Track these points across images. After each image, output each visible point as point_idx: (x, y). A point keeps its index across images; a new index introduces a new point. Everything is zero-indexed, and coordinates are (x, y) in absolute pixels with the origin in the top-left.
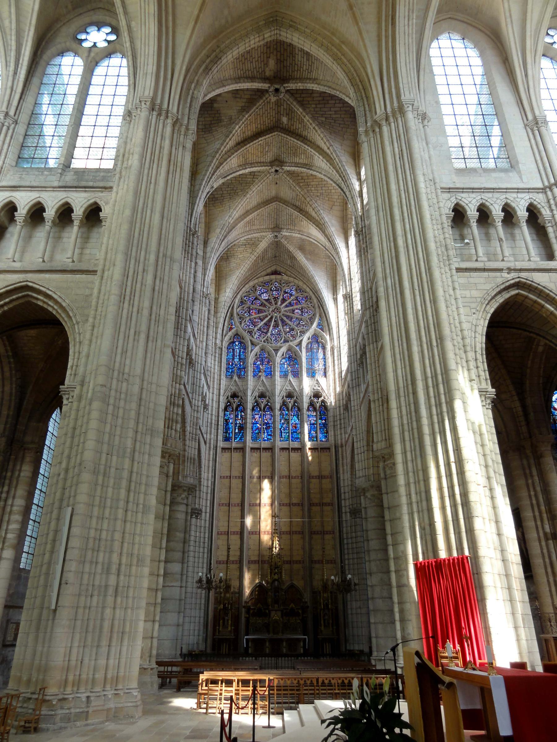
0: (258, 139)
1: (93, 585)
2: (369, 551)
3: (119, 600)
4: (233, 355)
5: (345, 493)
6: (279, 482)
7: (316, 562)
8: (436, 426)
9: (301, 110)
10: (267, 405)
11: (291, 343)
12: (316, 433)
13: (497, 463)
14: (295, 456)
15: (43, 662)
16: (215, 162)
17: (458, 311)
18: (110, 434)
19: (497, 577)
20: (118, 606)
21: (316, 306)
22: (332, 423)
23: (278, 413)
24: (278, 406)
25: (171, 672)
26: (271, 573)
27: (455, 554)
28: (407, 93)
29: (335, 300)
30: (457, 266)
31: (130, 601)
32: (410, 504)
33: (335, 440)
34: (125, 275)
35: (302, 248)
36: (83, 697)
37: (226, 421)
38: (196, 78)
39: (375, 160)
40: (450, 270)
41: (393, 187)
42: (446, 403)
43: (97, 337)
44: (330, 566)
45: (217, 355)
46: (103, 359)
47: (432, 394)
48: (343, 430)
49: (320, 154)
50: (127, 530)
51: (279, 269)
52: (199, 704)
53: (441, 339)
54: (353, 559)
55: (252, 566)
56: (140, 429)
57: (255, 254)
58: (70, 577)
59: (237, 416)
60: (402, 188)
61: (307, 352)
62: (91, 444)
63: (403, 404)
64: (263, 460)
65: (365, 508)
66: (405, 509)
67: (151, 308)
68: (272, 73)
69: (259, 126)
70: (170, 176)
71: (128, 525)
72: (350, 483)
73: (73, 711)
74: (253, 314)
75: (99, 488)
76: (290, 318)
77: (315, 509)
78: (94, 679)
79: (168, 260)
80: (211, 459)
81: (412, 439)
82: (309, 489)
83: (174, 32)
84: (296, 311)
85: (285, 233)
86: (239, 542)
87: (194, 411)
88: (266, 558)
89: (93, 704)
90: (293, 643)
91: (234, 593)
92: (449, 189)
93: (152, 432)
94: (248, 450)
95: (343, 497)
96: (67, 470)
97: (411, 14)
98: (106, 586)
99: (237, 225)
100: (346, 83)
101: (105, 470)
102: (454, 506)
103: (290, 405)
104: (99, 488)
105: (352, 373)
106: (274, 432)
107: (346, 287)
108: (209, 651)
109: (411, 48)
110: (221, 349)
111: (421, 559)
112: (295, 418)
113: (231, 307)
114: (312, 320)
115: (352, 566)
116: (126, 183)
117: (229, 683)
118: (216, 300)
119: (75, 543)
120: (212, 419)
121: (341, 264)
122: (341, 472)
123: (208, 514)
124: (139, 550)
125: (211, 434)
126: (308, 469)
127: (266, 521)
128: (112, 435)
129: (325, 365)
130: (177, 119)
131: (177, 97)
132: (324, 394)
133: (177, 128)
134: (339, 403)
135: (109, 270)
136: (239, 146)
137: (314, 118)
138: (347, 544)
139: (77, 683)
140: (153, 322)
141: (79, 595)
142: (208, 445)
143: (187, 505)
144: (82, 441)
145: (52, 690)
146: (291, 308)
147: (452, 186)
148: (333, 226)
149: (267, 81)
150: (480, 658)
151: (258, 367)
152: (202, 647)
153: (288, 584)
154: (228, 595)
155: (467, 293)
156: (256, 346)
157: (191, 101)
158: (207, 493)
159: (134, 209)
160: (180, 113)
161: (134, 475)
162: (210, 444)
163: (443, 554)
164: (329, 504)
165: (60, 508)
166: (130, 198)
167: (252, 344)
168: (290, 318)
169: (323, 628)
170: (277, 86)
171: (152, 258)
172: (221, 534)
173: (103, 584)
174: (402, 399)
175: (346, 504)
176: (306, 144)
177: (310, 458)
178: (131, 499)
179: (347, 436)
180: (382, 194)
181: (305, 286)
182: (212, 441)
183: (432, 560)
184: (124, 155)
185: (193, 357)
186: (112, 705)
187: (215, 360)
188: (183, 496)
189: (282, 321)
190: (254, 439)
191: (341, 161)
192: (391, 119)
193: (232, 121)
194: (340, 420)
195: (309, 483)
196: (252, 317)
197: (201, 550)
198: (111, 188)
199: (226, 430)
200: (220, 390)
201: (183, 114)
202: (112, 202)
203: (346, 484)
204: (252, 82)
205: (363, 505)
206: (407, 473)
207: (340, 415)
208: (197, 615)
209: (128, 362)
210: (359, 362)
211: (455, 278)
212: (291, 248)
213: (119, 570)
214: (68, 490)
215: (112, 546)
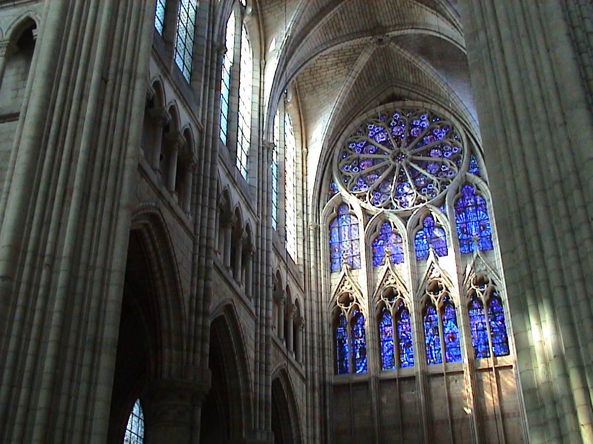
51: (397, 91)
80: (317, 405)
84: (433, 151)
120: (312, 342)
125: (313, 364)
181: (442, 111)
189: (412, 170)
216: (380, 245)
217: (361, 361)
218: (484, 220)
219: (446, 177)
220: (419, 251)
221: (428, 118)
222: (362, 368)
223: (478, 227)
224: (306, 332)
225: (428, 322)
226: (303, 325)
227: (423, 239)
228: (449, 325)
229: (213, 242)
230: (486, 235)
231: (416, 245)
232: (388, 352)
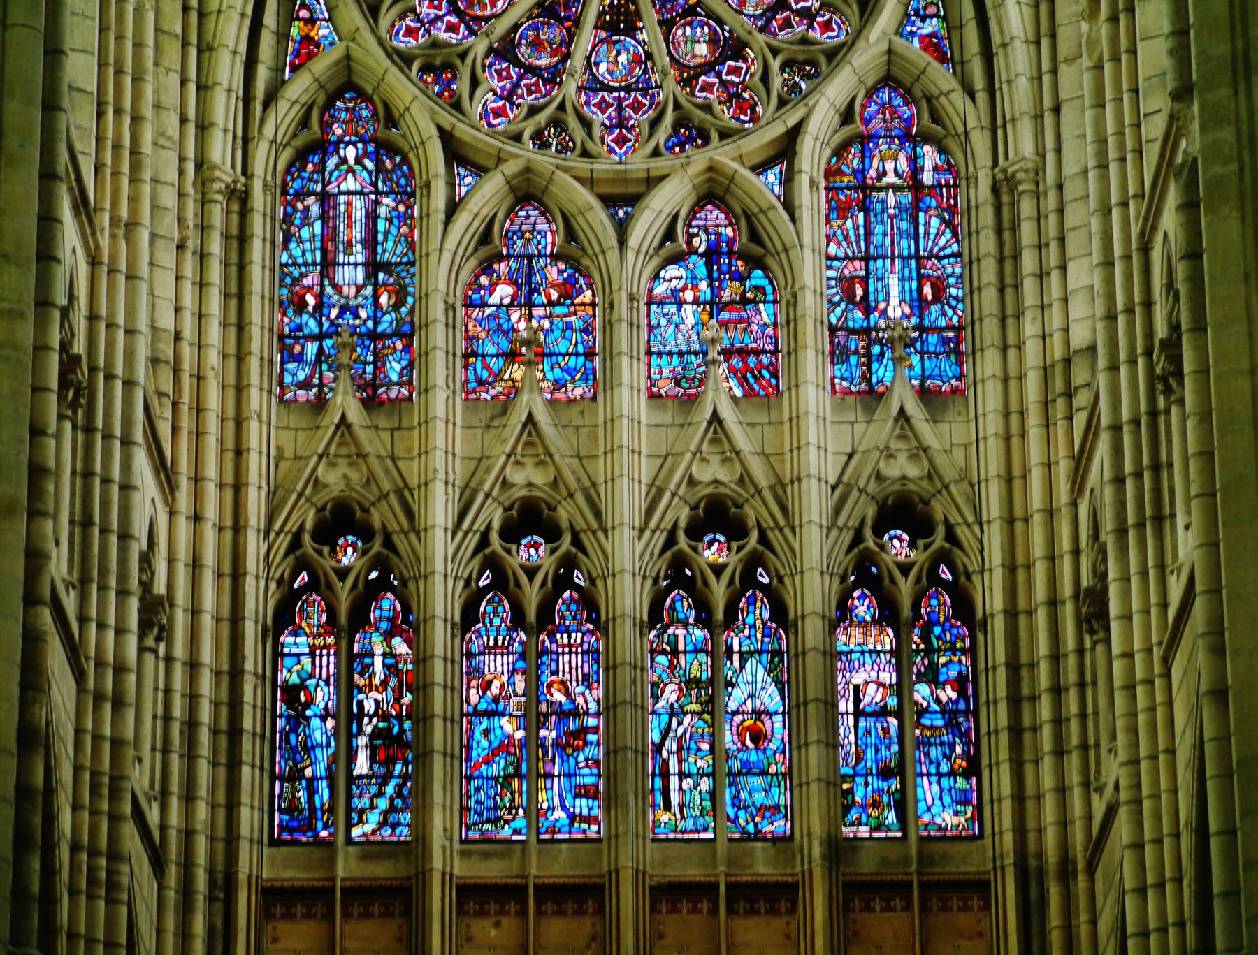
4: (329, 235)
10: (562, 581)
11: (722, 154)
22: (1002, 716)
33: (1020, 830)
48: (1074, 761)
59: (354, 662)
87: (99, 698)
103: (719, 592)
110: (240, 198)
112: (755, 670)
120: (192, 698)
125: (189, 797)
142: (172, 873)
156: (480, 171)
162: (187, 864)
167: (456, 153)
179: (1099, 808)
182: (201, 845)
185: (79, 347)
187: (202, 285)
194: (1057, 690)
200: (238, 487)
207: (1056, 658)
216: (500, 306)
217: (374, 789)
218: (940, 259)
219: (804, 41)
220: (660, 354)
222: (373, 818)
223: (914, 285)
224: (169, 659)
225: (663, 652)
226: (162, 628)
227: (680, 304)
228: (747, 674)
229: (52, 443)
230: (942, 322)
231: (651, 328)
232: (488, 761)
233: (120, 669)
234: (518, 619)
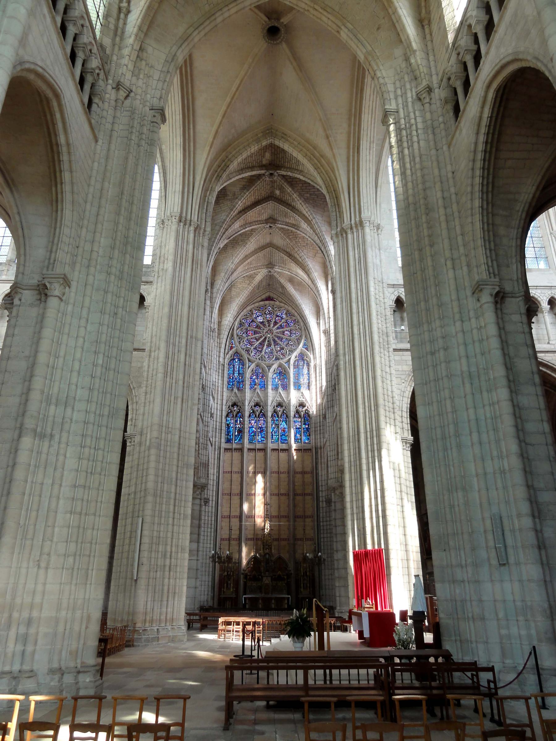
0: (256, 207)
1: (157, 565)
2: (336, 534)
3: (172, 573)
5: (322, 486)
6: (271, 477)
7: (298, 540)
8: (371, 465)
9: (290, 189)
10: (261, 412)
11: (281, 361)
12: (301, 436)
13: (410, 487)
14: (283, 455)
15: (131, 609)
16: (222, 230)
17: (391, 383)
18: (162, 470)
19: (400, 562)
20: (171, 577)
21: (303, 328)
23: (270, 420)
24: (270, 414)
25: (193, 620)
26: (263, 548)
27: (376, 547)
28: (366, 211)
29: (318, 324)
30: (395, 347)
31: (178, 574)
32: (352, 514)
33: (315, 443)
34: (167, 357)
35: (291, 280)
36: (155, 629)
37: (228, 426)
38: (211, 186)
39: (342, 260)
40: (388, 352)
41: (353, 285)
42: (378, 450)
43: (150, 402)
44: (309, 543)
45: (220, 371)
46: (156, 420)
47: (369, 443)
48: (322, 435)
49: (305, 221)
50: (175, 531)
51: (272, 295)
52: (219, 637)
53: (377, 406)
54: (327, 537)
55: (249, 542)
56: (180, 465)
57: (252, 285)
58: (145, 560)
59: (236, 421)
60: (359, 287)
61: (294, 368)
62: (151, 478)
63: (352, 448)
64: (257, 458)
65: (335, 502)
66: (349, 517)
67: (184, 377)
68: (268, 162)
69: (257, 197)
70: (194, 273)
71: (175, 527)
72: (326, 478)
73: (150, 636)
74: (250, 335)
75: (158, 505)
76: (281, 339)
77: (299, 498)
78: (160, 620)
79: (194, 340)
80: (216, 458)
81: (356, 472)
82: (294, 482)
83: (194, 153)
84: (286, 332)
85: (277, 269)
86: (238, 524)
88: (260, 537)
89: (161, 633)
90: (280, 601)
91: (235, 563)
92: (394, 285)
93: (187, 466)
94: (245, 450)
95: (320, 489)
96: (135, 493)
97: (372, 145)
98: (164, 566)
99: (237, 268)
100: (323, 187)
101: (160, 494)
102: (378, 517)
103: (280, 414)
104: (158, 505)
105: (328, 395)
106: (267, 436)
107: (325, 324)
108: (216, 606)
109: (371, 172)
111: (357, 549)
113: (232, 329)
114: (298, 341)
115: (326, 543)
116: (163, 283)
117: (238, 624)
118: (220, 323)
119: (146, 540)
120: (216, 425)
121: (322, 304)
122: (320, 469)
123: (214, 502)
124: (182, 543)
125: (216, 437)
126: (293, 466)
127: (259, 507)
128: (163, 470)
129: (309, 379)
130: (198, 225)
131: (197, 207)
132: (307, 405)
133: (197, 232)
134: (320, 412)
135: (155, 351)
136: (241, 214)
137: (301, 195)
138: (323, 526)
139: (152, 621)
140: (185, 388)
141: (150, 571)
142: (213, 446)
143: (201, 499)
144: (145, 474)
145: (139, 625)
146: (282, 330)
147: (396, 283)
148: (316, 271)
149: (264, 168)
150: (385, 608)
151: (254, 381)
152: (210, 604)
153: (277, 556)
154: (230, 565)
155: (400, 368)
156: (252, 363)
157: (207, 206)
158: (213, 485)
159: (171, 306)
160: (199, 220)
161: (177, 495)
162: (215, 446)
163: (369, 547)
164: (309, 495)
165: (133, 517)
166: (167, 297)
167: (249, 361)
168: (281, 339)
169: (302, 590)
170: (271, 172)
171: (184, 341)
172: (225, 518)
173: (162, 564)
174: (351, 444)
175: (323, 495)
176: (294, 212)
177: (295, 457)
178: (176, 511)
179: (325, 440)
180: (346, 289)
181: (293, 311)
183: (363, 550)
184: (160, 257)
186: (171, 634)
188: (198, 492)
189: (274, 340)
190: (250, 442)
191: (321, 232)
192: (355, 230)
193: (235, 197)
194: (320, 426)
195: (294, 477)
196: (249, 337)
197: (209, 530)
198: (151, 282)
199: (228, 433)
200: (222, 400)
201: (201, 219)
202: (153, 295)
203: (323, 479)
204: (252, 171)
205: (333, 500)
206: (352, 494)
207: (320, 422)
208: (207, 580)
209: (171, 420)
210: (333, 388)
211: (391, 358)
212: (282, 281)
213: (171, 556)
214: (137, 506)
215: (166, 541)
221: (286, 314)
233: (208, 422)
234: (256, 416)
